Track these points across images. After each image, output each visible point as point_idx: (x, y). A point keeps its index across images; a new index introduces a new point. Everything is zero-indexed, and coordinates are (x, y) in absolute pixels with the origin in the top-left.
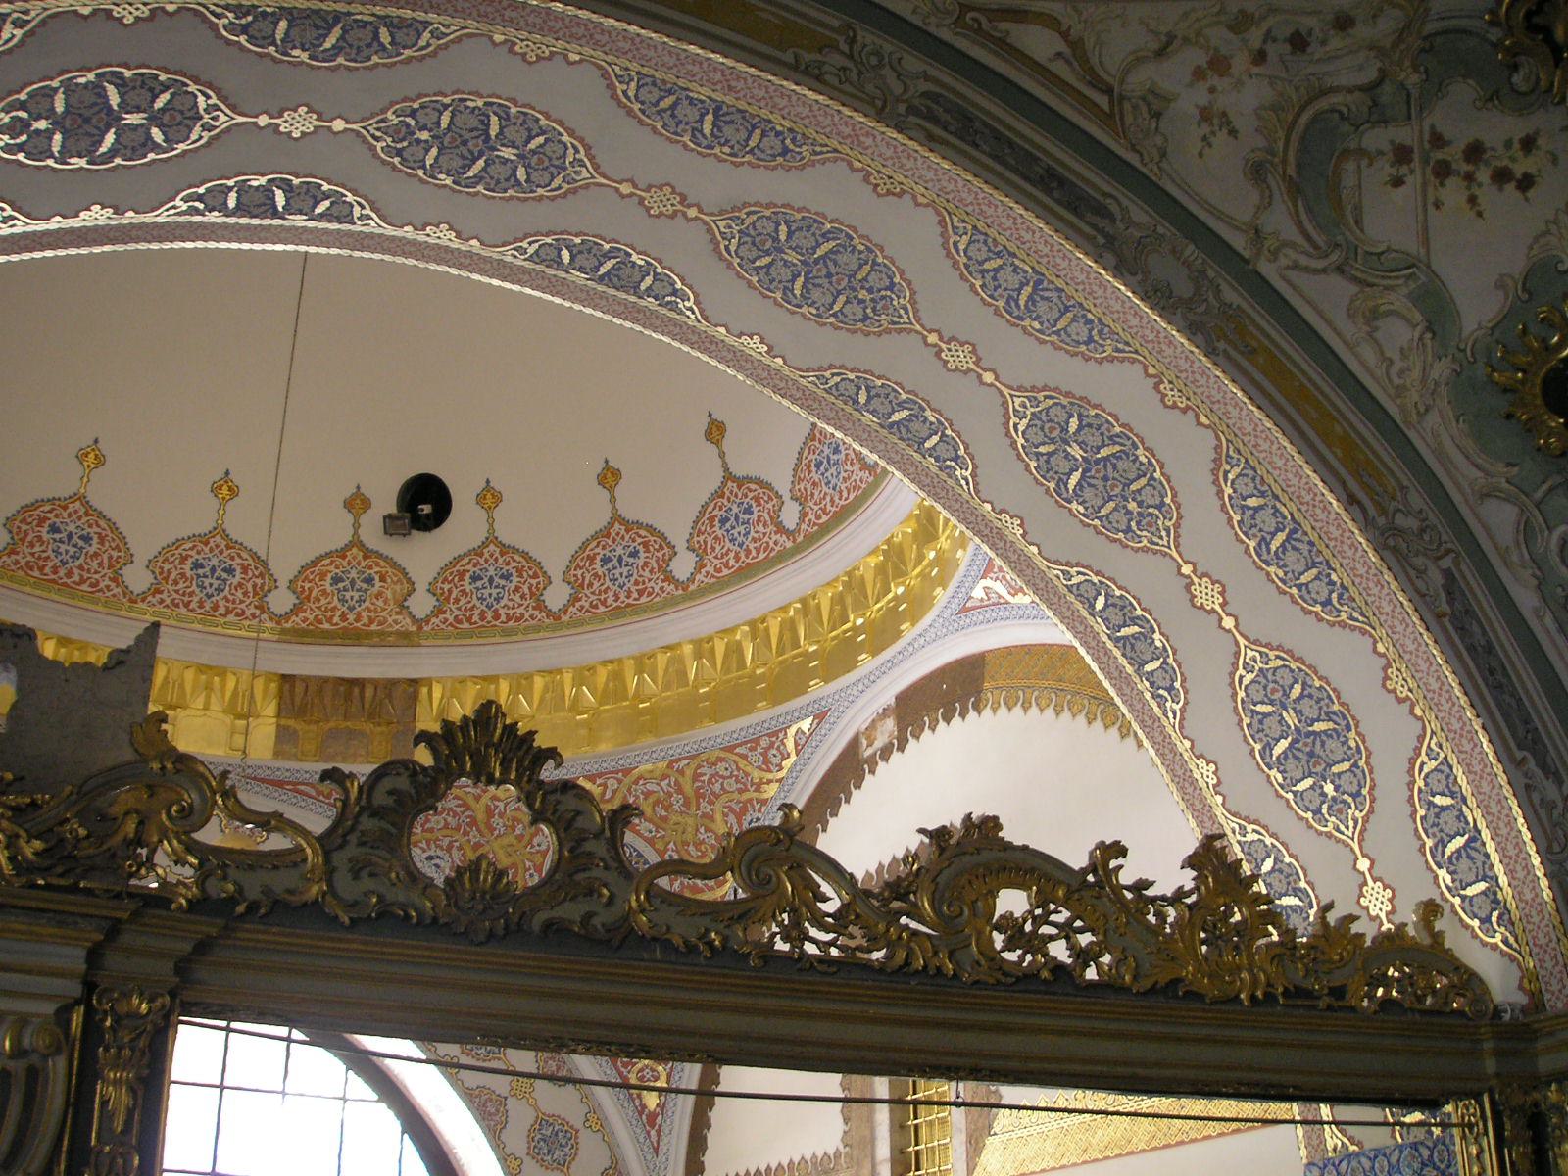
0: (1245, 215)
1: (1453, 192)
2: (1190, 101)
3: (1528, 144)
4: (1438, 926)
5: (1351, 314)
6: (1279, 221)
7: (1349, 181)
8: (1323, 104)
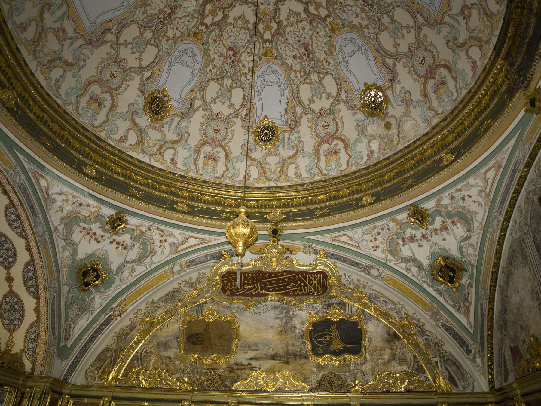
0: (56, 225)
1: (88, 237)
2: (58, 204)
3: (102, 237)
4: (23, 354)
5: (62, 247)
6: (60, 228)
7: (74, 228)
8: (78, 215)
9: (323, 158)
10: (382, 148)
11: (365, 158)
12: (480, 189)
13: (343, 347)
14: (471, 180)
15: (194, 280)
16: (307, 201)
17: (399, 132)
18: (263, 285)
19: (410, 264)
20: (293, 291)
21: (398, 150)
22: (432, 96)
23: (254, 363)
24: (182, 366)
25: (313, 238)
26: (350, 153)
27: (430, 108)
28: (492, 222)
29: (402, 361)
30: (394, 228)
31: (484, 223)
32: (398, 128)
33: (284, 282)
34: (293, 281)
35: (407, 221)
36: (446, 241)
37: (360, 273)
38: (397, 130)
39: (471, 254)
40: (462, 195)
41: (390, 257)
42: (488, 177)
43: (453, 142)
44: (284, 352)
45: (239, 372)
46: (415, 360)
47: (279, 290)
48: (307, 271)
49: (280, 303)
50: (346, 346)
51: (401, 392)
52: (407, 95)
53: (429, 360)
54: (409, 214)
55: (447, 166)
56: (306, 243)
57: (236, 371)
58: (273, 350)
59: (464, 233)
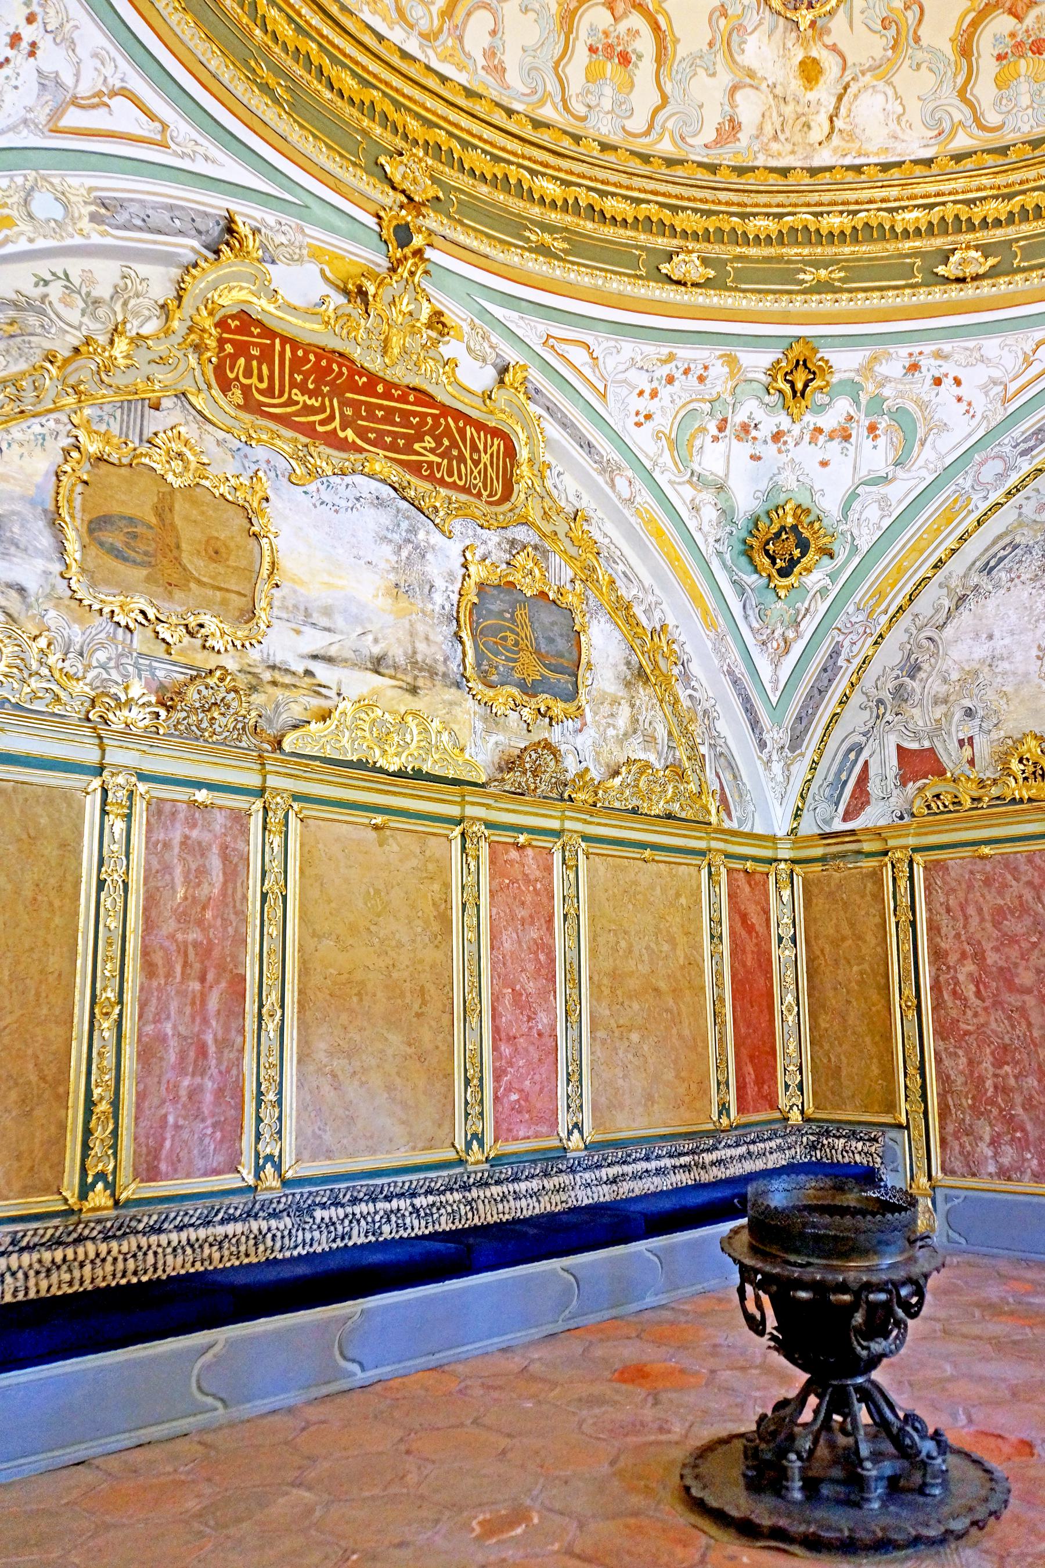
9: (581, 55)
10: (768, 130)
11: (709, 135)
12: (997, 374)
13: (542, 675)
14: (991, 345)
15: (103, 291)
16: (506, 176)
17: (837, 108)
18: (349, 412)
19: (707, 496)
20: (430, 464)
21: (816, 163)
22: (987, 66)
23: (322, 671)
24: (77, 635)
25: (498, 312)
26: (668, 88)
27: (962, 94)
28: (982, 464)
29: (650, 740)
30: (719, 382)
32: (840, 98)
33: (410, 426)
34: (431, 432)
35: (765, 379)
37: (594, 474)
38: (834, 100)
39: (868, 524)
40: (943, 370)
41: (666, 458)
43: (998, 223)
44: (405, 654)
45: (279, 693)
46: (671, 744)
47: (393, 448)
48: (474, 414)
49: (393, 494)
50: (547, 673)
51: (658, 816)
52: (909, 14)
53: (694, 748)
54: (778, 362)
55: (961, 280)
56: (476, 321)
57: (271, 689)
58: (376, 641)
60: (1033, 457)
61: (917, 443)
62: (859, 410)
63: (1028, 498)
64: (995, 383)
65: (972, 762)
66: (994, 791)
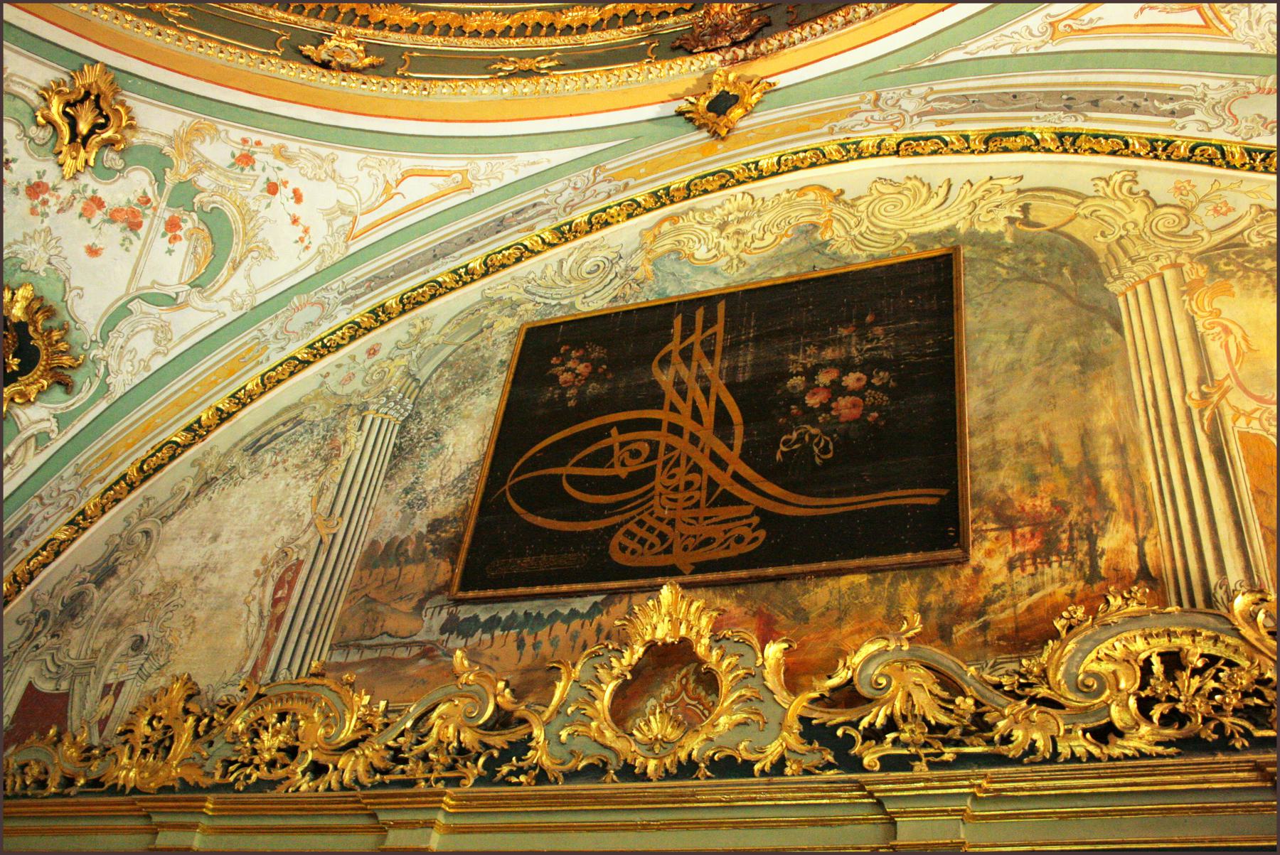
12: (348, 200)
14: (348, 161)
28: (298, 309)
31: (261, 298)
36: (96, 260)
40: (282, 175)
42: (401, 188)
55: (325, 65)
59: (175, 280)
60: (355, 306)
61: (228, 265)
62: (160, 195)
63: (339, 366)
64: (343, 212)
65: (103, 723)
66: (95, 768)
